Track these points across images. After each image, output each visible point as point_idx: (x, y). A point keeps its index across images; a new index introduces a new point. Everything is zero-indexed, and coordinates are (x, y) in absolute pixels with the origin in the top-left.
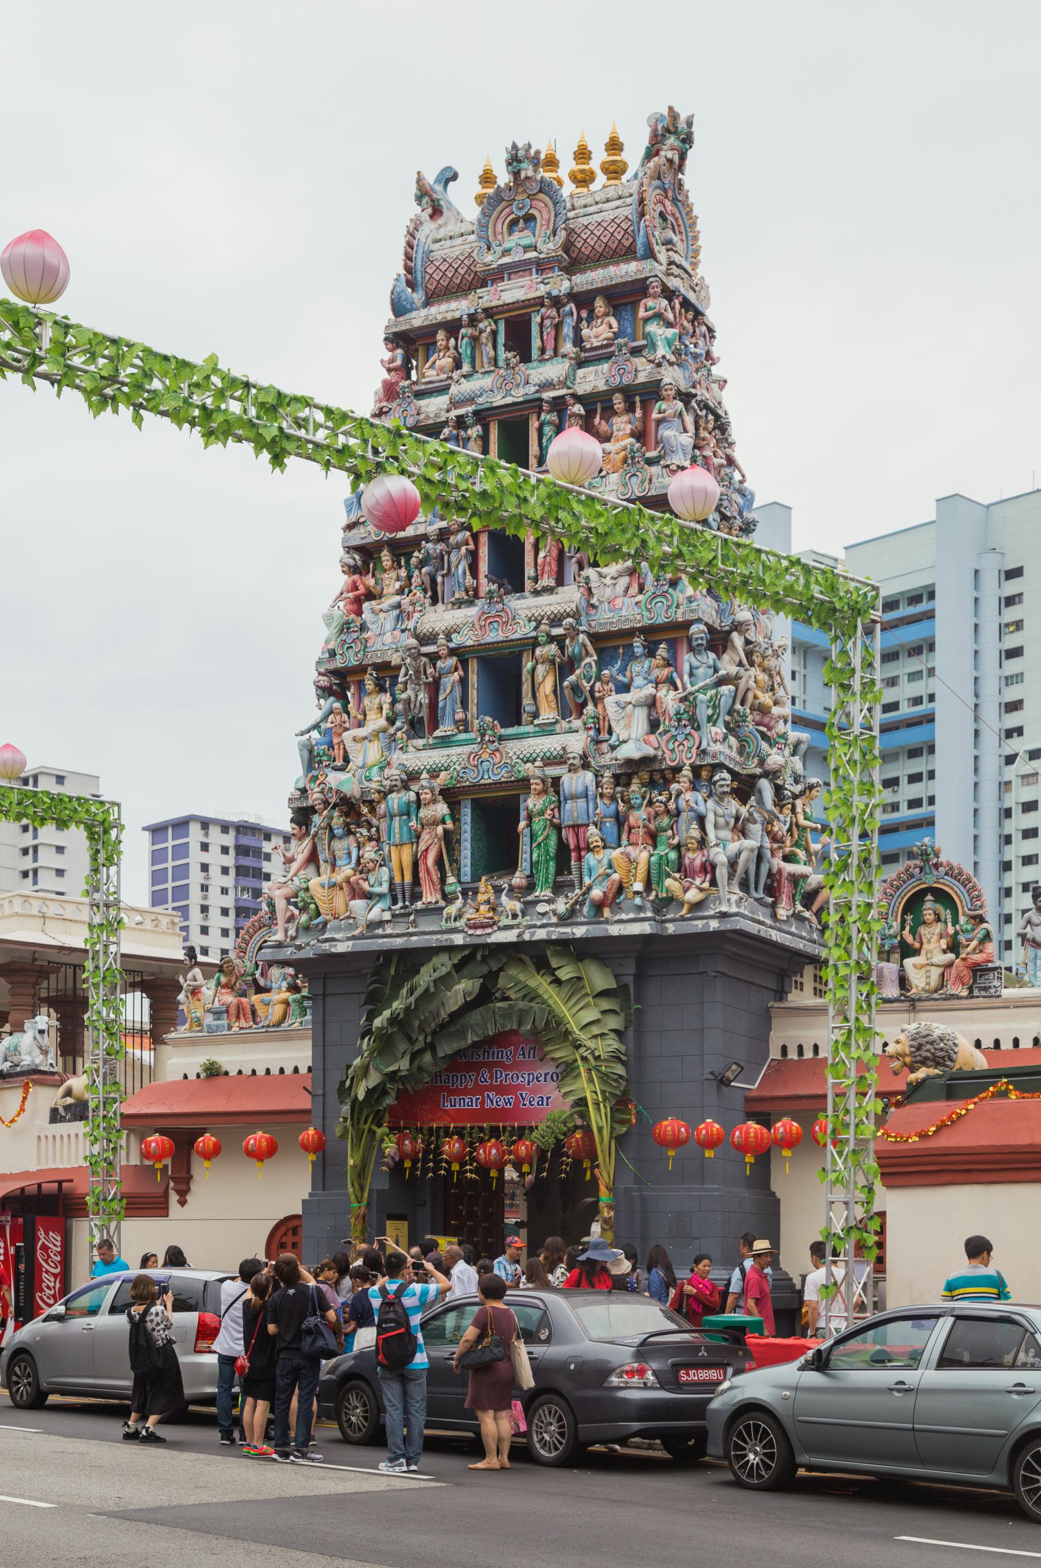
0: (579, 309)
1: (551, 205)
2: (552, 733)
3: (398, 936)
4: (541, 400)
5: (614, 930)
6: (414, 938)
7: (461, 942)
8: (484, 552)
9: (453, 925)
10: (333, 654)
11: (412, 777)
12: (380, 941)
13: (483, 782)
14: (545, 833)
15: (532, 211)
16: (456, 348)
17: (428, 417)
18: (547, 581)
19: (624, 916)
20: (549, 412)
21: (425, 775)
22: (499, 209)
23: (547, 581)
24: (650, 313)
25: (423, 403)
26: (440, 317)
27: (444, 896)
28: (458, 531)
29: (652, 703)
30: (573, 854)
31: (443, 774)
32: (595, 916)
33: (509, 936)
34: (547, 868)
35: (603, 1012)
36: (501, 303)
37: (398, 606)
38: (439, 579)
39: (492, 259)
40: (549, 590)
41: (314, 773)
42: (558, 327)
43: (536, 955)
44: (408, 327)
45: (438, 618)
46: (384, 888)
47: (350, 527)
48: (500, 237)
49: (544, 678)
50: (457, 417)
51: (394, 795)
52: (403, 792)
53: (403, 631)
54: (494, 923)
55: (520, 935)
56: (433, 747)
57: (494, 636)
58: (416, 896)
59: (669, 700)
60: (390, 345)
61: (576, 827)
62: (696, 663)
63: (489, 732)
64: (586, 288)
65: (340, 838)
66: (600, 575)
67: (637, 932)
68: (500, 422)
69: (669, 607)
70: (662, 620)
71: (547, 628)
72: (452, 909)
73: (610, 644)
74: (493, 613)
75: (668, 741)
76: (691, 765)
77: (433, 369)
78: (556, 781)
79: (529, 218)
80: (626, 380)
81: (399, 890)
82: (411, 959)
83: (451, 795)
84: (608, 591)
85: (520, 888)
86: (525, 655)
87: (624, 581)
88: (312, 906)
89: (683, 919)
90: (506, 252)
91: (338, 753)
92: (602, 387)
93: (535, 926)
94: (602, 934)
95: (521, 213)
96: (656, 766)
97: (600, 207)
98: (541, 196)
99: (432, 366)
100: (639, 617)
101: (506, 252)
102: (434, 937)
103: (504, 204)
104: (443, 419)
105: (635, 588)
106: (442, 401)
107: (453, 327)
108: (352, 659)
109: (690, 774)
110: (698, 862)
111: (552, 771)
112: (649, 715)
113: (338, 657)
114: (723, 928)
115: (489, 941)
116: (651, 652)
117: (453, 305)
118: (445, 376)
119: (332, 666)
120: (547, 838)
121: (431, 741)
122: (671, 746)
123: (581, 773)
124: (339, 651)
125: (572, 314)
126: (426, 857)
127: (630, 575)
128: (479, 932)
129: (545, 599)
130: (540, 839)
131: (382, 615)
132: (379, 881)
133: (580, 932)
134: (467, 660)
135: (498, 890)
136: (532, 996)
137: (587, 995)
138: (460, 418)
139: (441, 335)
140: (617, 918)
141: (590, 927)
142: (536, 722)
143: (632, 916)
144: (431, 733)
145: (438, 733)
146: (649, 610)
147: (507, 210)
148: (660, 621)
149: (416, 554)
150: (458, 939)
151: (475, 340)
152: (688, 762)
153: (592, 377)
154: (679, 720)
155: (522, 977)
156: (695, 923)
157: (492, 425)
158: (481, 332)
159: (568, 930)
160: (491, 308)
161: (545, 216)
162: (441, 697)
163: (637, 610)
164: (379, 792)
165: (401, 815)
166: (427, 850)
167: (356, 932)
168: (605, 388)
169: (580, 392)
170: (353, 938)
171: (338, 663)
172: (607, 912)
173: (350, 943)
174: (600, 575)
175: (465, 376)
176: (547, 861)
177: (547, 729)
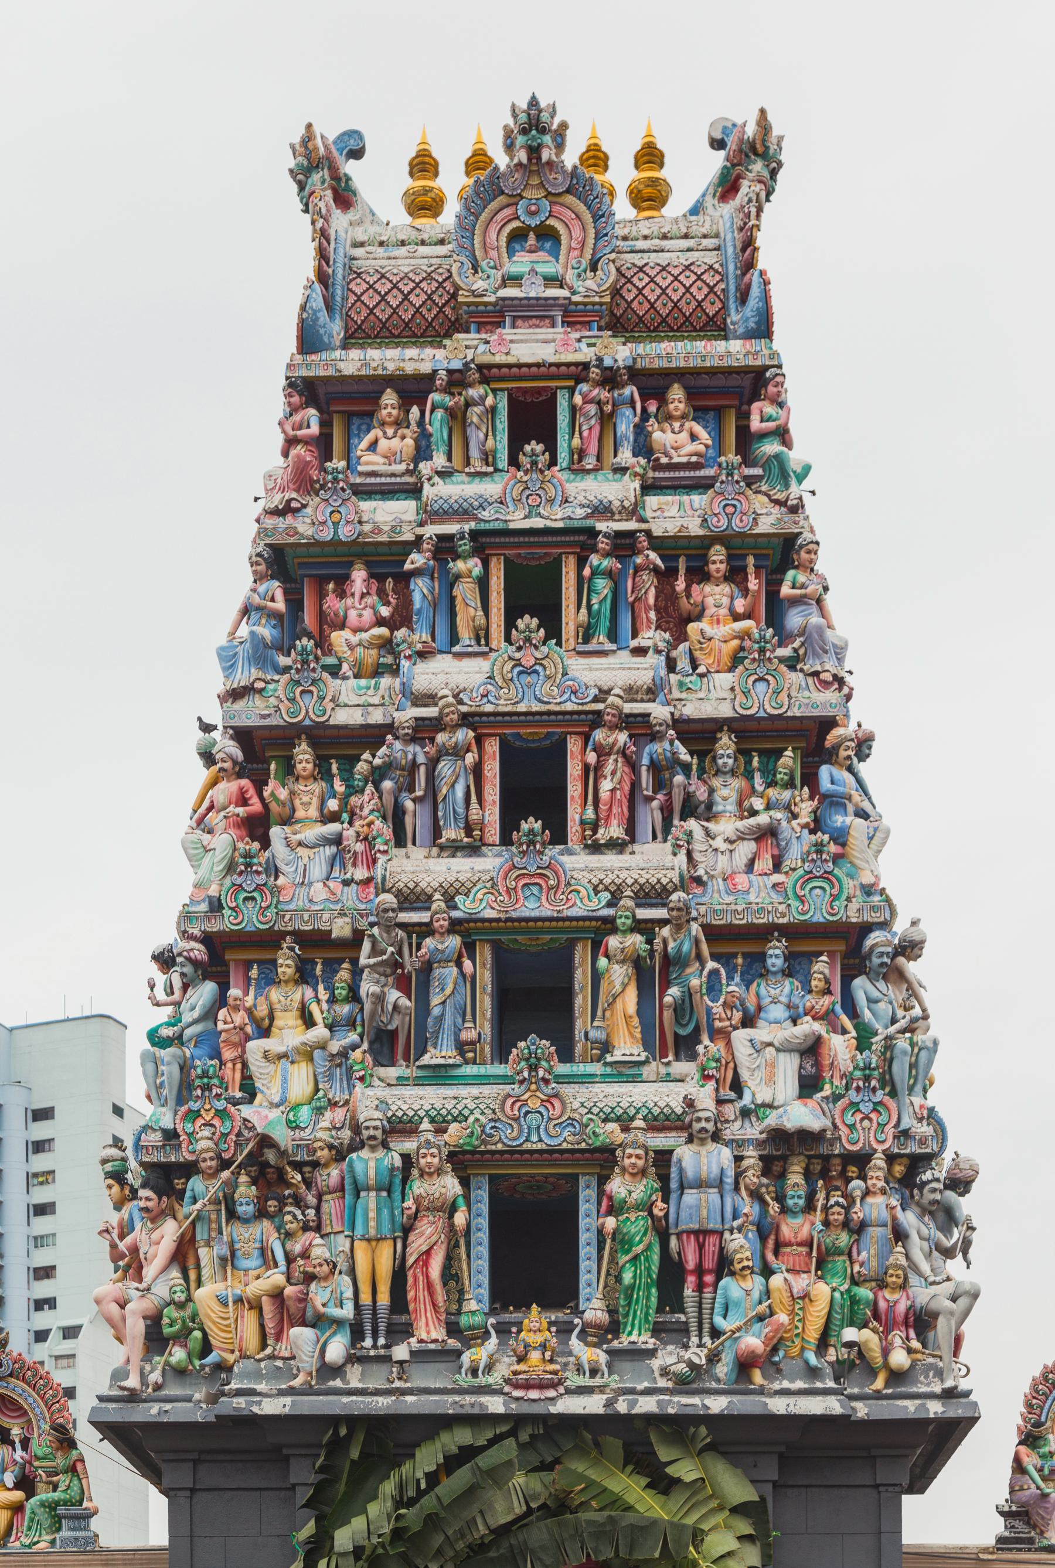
0: (644, 398)
1: (587, 217)
2: (635, 1079)
3: (377, 1392)
4: (592, 533)
5: (778, 1406)
6: (410, 1399)
7: (501, 1410)
8: (492, 769)
9: (482, 1380)
10: (216, 906)
11: (400, 1127)
12: (345, 1399)
13: (527, 1146)
14: (646, 1240)
15: (551, 222)
17: (377, 530)
18: (615, 830)
19: (786, 1384)
20: (607, 555)
21: (425, 1125)
22: (493, 205)
23: (615, 830)
24: (771, 425)
25: (366, 505)
26: (391, 367)
27: (453, 1329)
28: (456, 727)
29: (812, 1050)
30: (691, 1279)
31: (454, 1128)
32: (736, 1382)
33: (593, 1405)
34: (648, 1299)
35: (740, 1538)
36: (511, 360)
37: (337, 840)
38: (409, 805)
39: (483, 286)
40: (616, 846)
41: (194, 1105)
42: (606, 420)
43: (635, 1441)
44: (330, 372)
45: (418, 867)
46: (347, 1312)
47: (235, 694)
48: (494, 254)
49: (625, 986)
50: (442, 538)
51: (365, 1153)
52: (380, 1153)
53: (346, 883)
54: (560, 1382)
55: (609, 1404)
56: (418, 1082)
57: (531, 907)
58: (405, 1331)
59: (840, 1047)
60: (296, 399)
61: (701, 1234)
62: (875, 994)
63: (544, 1063)
64: (657, 364)
65: (246, 1221)
66: (708, 833)
67: (782, 1411)
68: (508, 563)
69: (835, 897)
70: (819, 916)
71: (630, 903)
72: (480, 1354)
73: (740, 944)
74: (532, 869)
75: (843, 1111)
76: (884, 1151)
77: (382, 450)
78: (663, 1159)
79: (547, 235)
80: (737, 525)
81: (367, 1316)
82: (388, 1438)
83: (461, 1161)
84: (723, 861)
85: (597, 1326)
86: (579, 947)
87: (746, 849)
88: (197, 1334)
89: (878, 1395)
90: (515, 280)
91: (232, 1075)
92: (695, 529)
93: (632, 1391)
94: (758, 1411)
95: (534, 222)
96: (824, 1150)
97: (673, 236)
98: (570, 199)
99: (373, 446)
100: (782, 908)
101: (515, 280)
102: (450, 1399)
103: (501, 200)
104: (409, 537)
105: (765, 863)
106: (405, 509)
107: (413, 389)
108: (253, 919)
109: (882, 1164)
110: (902, 1307)
111: (659, 1141)
112: (801, 1067)
113: (227, 912)
114: (951, 1414)
115: (553, 1410)
116: (796, 966)
117: (412, 352)
118: (402, 467)
119: (214, 927)
120: (649, 1247)
121: (407, 1072)
122: (849, 1119)
123: (711, 1146)
124: (228, 902)
125: (632, 403)
126: (426, 1264)
127: (757, 840)
128: (534, 1394)
129: (610, 859)
130: (639, 1249)
131: (302, 851)
132: (331, 1297)
133: (717, 1405)
134: (474, 943)
135: (564, 1330)
136: (617, 1503)
137: (721, 1508)
138: (444, 538)
139: (389, 398)
140: (776, 1386)
141: (735, 1398)
142: (609, 1058)
143: (800, 1384)
144: (417, 1060)
145: (426, 1059)
146: (801, 899)
147: (507, 212)
148: (818, 918)
149: (367, 756)
150: (495, 1405)
151: (457, 417)
152: (880, 1148)
153: (673, 511)
154: (867, 1079)
155: (593, 1474)
156: (901, 1403)
157: (494, 561)
158: (468, 404)
159: (696, 1400)
160: (490, 366)
161: (577, 233)
162: (435, 1000)
163: (776, 898)
164: (331, 1147)
165: (379, 1189)
166: (428, 1253)
167: (296, 1383)
168: (701, 532)
169: (657, 532)
170: (291, 1391)
171: (227, 922)
172: (758, 1377)
173: (288, 1400)
174: (708, 833)
175: (440, 474)
176: (648, 1287)
177: (627, 1072)
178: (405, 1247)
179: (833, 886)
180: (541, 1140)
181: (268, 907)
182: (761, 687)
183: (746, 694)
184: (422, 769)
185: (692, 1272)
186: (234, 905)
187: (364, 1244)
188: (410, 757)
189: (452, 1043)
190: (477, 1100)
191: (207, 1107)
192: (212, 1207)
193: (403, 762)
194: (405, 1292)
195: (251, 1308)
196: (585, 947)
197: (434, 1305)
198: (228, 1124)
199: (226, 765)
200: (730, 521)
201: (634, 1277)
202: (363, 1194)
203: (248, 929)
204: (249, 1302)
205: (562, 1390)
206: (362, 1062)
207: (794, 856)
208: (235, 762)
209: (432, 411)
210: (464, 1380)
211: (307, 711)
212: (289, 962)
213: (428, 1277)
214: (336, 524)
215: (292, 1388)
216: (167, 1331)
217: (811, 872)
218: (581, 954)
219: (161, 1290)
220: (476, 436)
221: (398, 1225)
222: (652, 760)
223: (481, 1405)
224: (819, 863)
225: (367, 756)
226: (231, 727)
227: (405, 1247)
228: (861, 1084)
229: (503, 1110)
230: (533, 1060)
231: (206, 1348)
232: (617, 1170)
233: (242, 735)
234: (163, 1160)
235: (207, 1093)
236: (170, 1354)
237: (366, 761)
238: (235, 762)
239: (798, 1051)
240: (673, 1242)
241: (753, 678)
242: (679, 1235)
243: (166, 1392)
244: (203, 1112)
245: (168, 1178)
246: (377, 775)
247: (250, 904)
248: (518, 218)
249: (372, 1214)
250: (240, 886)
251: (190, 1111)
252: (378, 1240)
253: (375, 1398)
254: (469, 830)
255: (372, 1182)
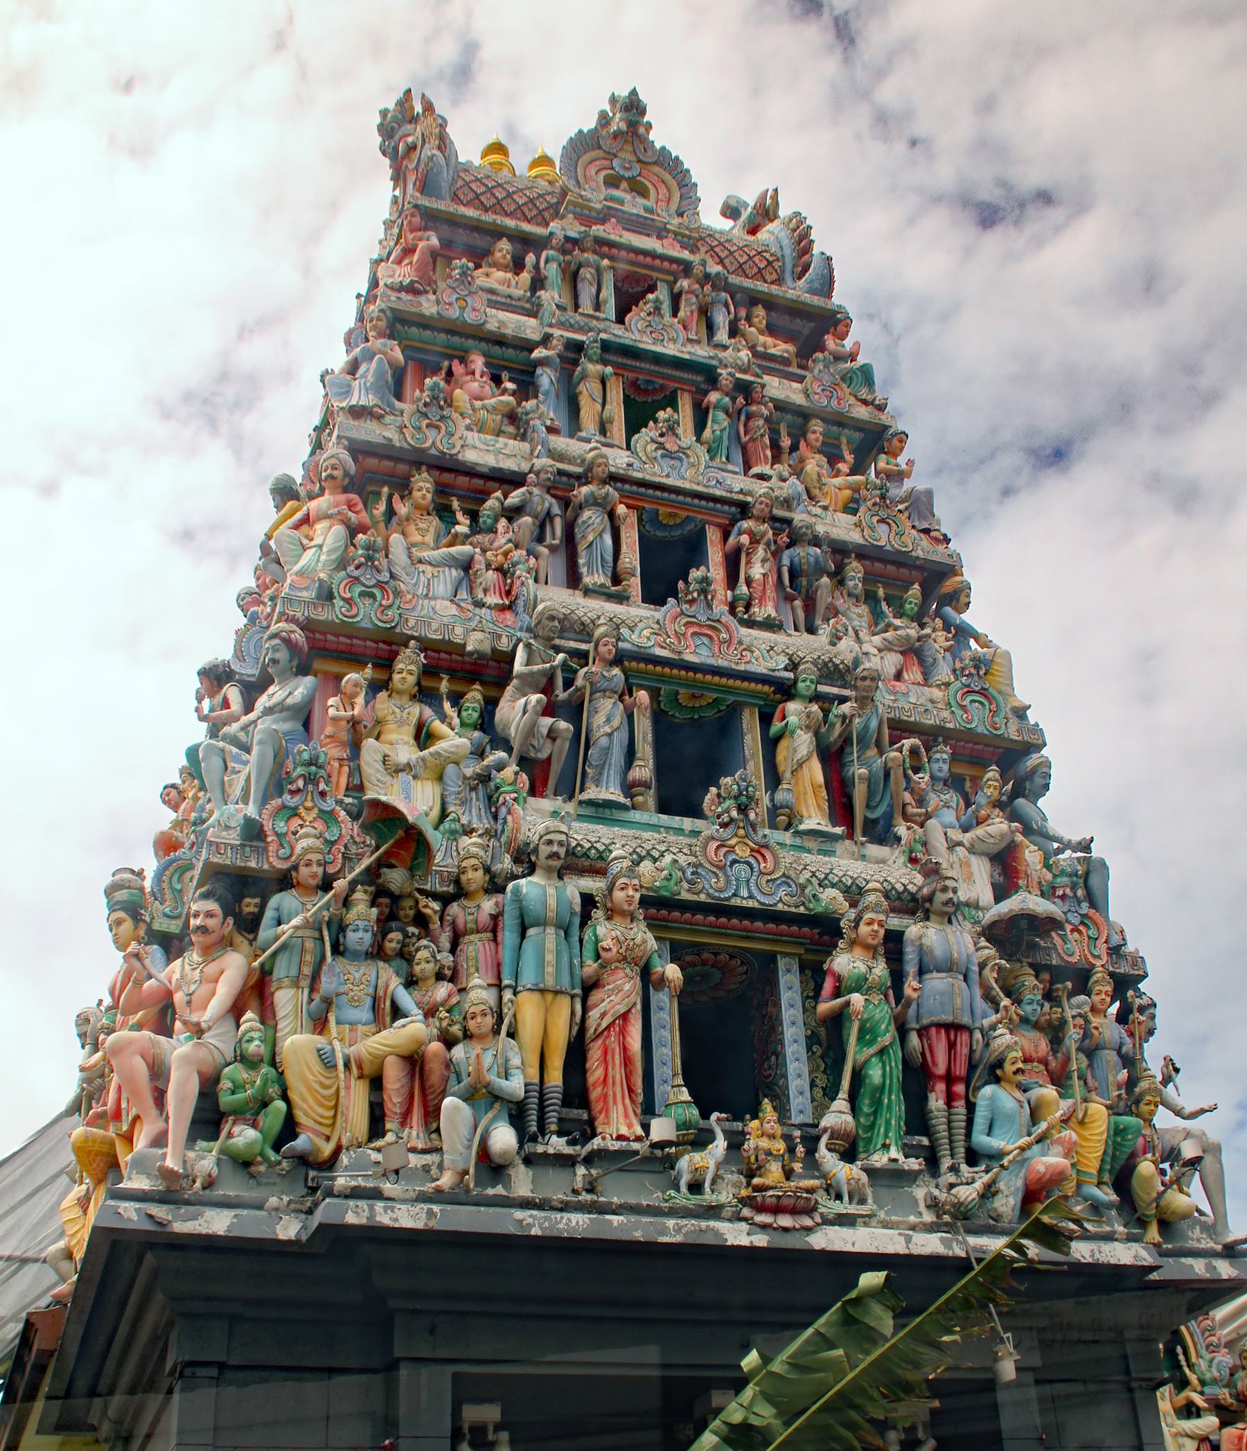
6: (616, 1219)
9: (708, 1197)
10: (327, 595)
16: (536, 267)
69: (994, 713)
108: (367, 615)
113: (338, 602)
124: (341, 590)
126: (623, 1033)
128: (785, 1221)
146: (963, 708)
149: (498, 494)
170: (438, 1196)
171: (336, 612)
178: (585, 1010)
179: (991, 704)
180: (751, 897)
181: (390, 607)
182: (884, 527)
183: (872, 529)
184: (558, 522)
185: (941, 1078)
186: (348, 595)
187: (536, 997)
188: (547, 505)
189: (618, 782)
190: (654, 849)
191: (309, 804)
192: (308, 933)
193: (539, 508)
194: (584, 1072)
195: (361, 1077)
196: (752, 714)
197: (631, 1090)
198: (336, 830)
199: (336, 473)
200: (829, 402)
201: (884, 1075)
202: (531, 932)
203: (363, 625)
204: (360, 1067)
205: (818, 1220)
206: (514, 783)
207: (943, 672)
208: (346, 474)
209: (546, 262)
210: (683, 1198)
211: (433, 441)
212: (412, 667)
213: (625, 1049)
214: (463, 309)
215: (439, 1191)
216: (226, 1100)
217: (969, 686)
218: (750, 722)
219: (220, 1042)
220: (586, 293)
221: (578, 981)
222: (792, 562)
223: (716, 1233)
224: (976, 678)
225: (498, 494)
226: (348, 439)
227: (585, 1010)
228: (1068, 891)
229: (705, 855)
230: (744, 799)
231: (290, 1128)
232: (841, 944)
233: (358, 450)
234: (239, 863)
235: (310, 787)
236: (230, 1135)
237: (498, 499)
238: (346, 474)
239: (987, 855)
240: (914, 1040)
241: (876, 518)
242: (923, 1032)
243: (219, 1192)
244: (302, 810)
245: (243, 893)
246: (512, 514)
247: (368, 601)
248: (612, 168)
249: (550, 957)
250: (357, 579)
251: (284, 807)
252: (556, 993)
253: (566, 1215)
254: (616, 580)
255: (551, 915)
